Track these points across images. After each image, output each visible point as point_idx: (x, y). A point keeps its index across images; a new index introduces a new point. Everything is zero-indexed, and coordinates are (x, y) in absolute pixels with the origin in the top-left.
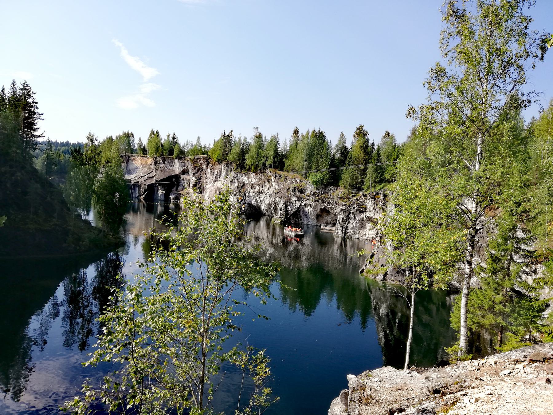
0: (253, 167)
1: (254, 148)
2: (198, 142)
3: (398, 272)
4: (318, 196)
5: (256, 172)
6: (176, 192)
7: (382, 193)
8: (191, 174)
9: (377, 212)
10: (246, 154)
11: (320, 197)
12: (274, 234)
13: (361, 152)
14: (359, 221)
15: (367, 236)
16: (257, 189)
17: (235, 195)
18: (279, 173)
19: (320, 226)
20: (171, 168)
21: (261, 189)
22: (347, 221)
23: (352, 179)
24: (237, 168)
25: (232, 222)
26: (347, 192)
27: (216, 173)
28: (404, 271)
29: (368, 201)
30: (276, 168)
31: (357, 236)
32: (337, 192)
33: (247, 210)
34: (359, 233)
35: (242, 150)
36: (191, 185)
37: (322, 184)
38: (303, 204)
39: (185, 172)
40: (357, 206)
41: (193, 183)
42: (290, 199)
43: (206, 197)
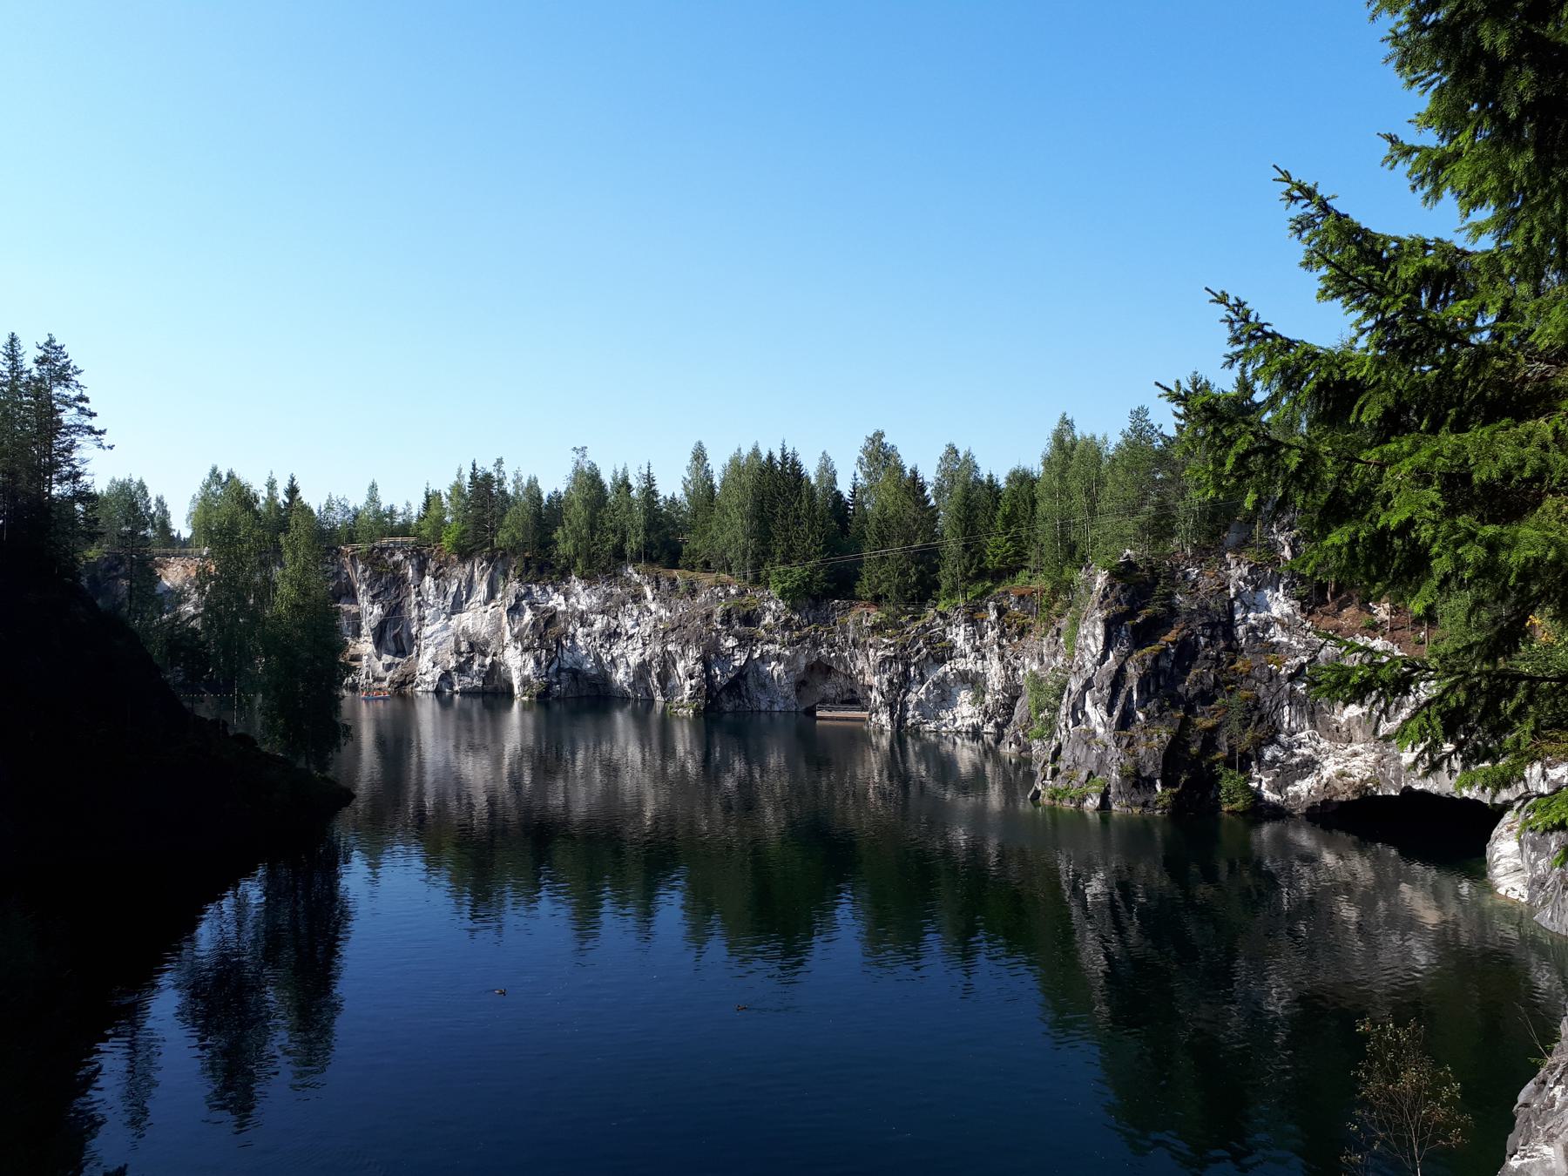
1: (578, 506)
2: (373, 499)
3: (1135, 785)
4: (799, 628)
5: (589, 579)
9: (984, 657)
12: (667, 749)
13: (909, 502)
16: (598, 626)
17: (526, 650)
19: (810, 712)
21: (614, 623)
24: (528, 568)
25: (516, 725)
27: (454, 588)
28: (1150, 782)
30: (651, 560)
31: (932, 726)
32: (851, 619)
34: (938, 718)
35: (538, 516)
36: (365, 630)
37: (808, 594)
38: (756, 656)
41: (374, 624)
42: (717, 643)
43: (424, 663)
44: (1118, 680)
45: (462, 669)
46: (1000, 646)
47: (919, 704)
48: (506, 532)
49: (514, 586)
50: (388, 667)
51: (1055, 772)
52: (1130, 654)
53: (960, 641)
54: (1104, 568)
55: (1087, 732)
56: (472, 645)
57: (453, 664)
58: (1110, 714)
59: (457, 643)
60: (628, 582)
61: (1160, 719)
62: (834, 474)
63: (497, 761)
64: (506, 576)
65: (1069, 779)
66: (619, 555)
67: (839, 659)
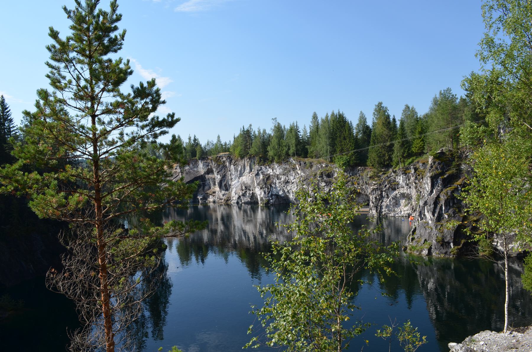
0: (276, 158)
2: (219, 140)
3: (442, 245)
5: (279, 163)
6: (203, 192)
7: (412, 167)
8: (215, 173)
9: (410, 187)
10: (267, 146)
11: (349, 179)
13: (385, 129)
14: (393, 198)
15: (402, 213)
16: (282, 179)
17: (261, 188)
18: (303, 160)
20: (196, 169)
21: (287, 178)
22: (380, 200)
23: (379, 157)
24: (260, 161)
25: (261, 215)
26: (376, 170)
27: (240, 169)
28: (449, 243)
29: (399, 178)
31: (392, 214)
33: (275, 202)
34: (394, 211)
36: (217, 184)
37: (349, 165)
39: (210, 171)
40: (388, 184)
41: (218, 181)
42: (318, 185)
43: (233, 194)
44: (436, 202)
45: (244, 195)
46: (415, 183)
47: (387, 206)
48: (257, 149)
49: (257, 167)
50: (224, 195)
51: (413, 239)
52: (442, 190)
53: (401, 182)
54: (431, 155)
55: (425, 223)
56: (246, 187)
57: (241, 194)
58: (434, 216)
59: (242, 187)
60: (291, 163)
61: (454, 217)
62: (366, 119)
63: (255, 226)
64: (254, 163)
65: (418, 242)
66: (288, 155)
67: (362, 189)
